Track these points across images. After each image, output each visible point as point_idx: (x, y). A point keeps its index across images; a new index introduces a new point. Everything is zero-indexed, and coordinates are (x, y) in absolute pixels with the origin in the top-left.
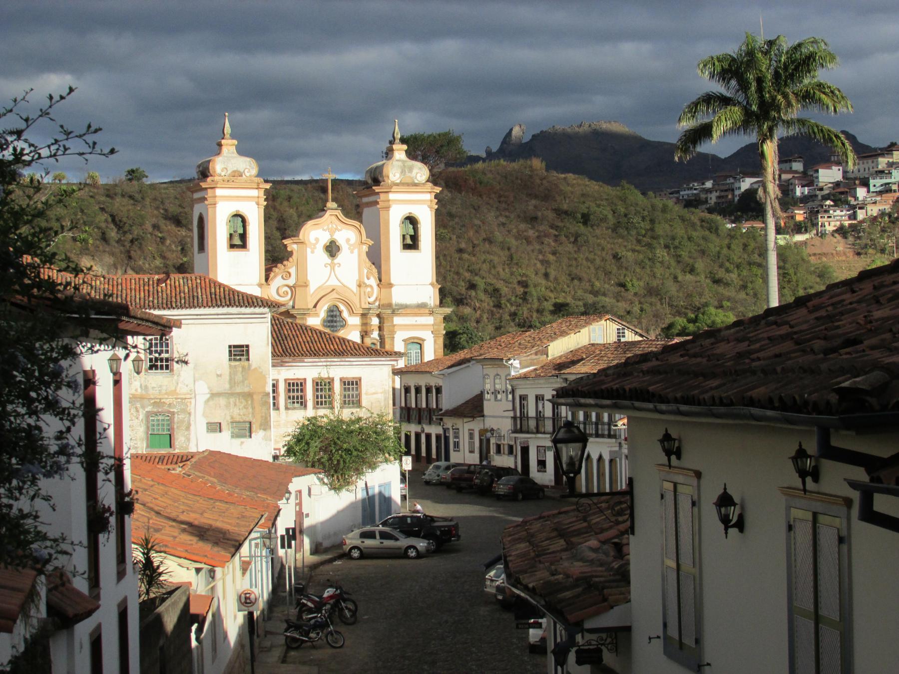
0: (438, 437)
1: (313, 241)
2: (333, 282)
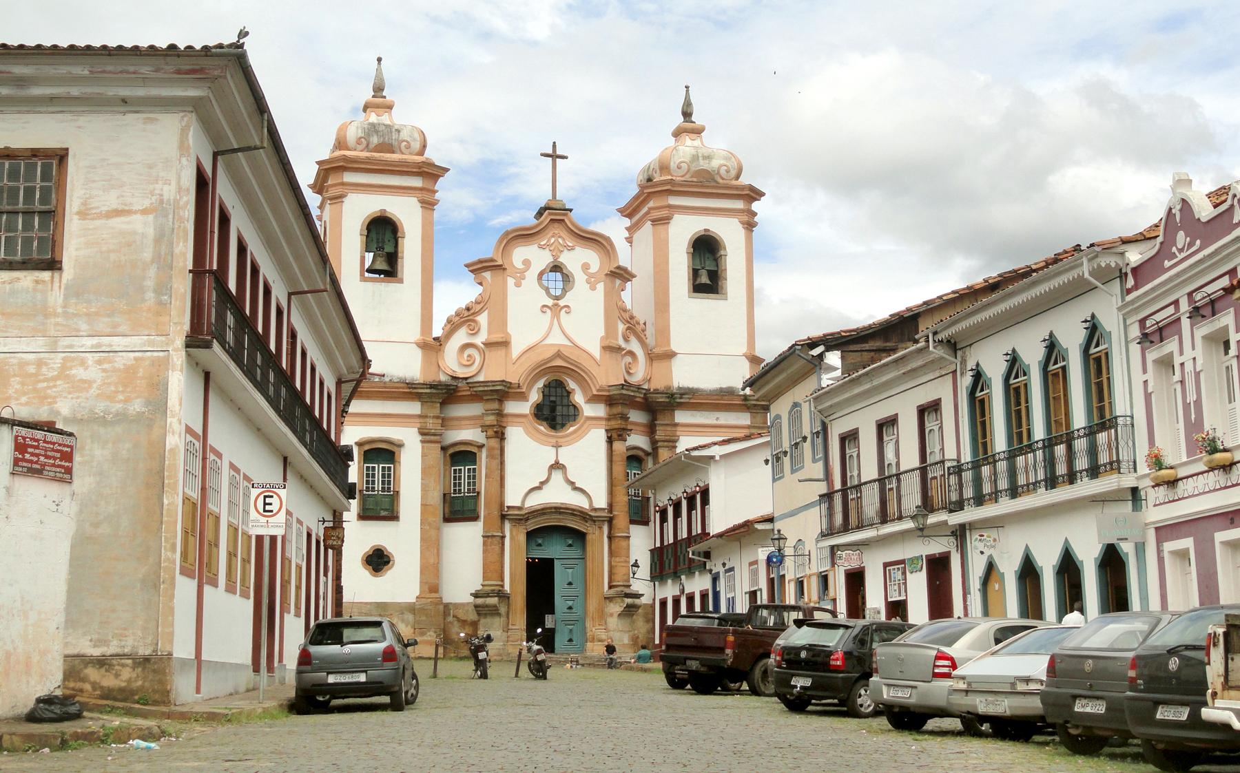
0: (704, 596)
1: (518, 264)
2: (556, 339)
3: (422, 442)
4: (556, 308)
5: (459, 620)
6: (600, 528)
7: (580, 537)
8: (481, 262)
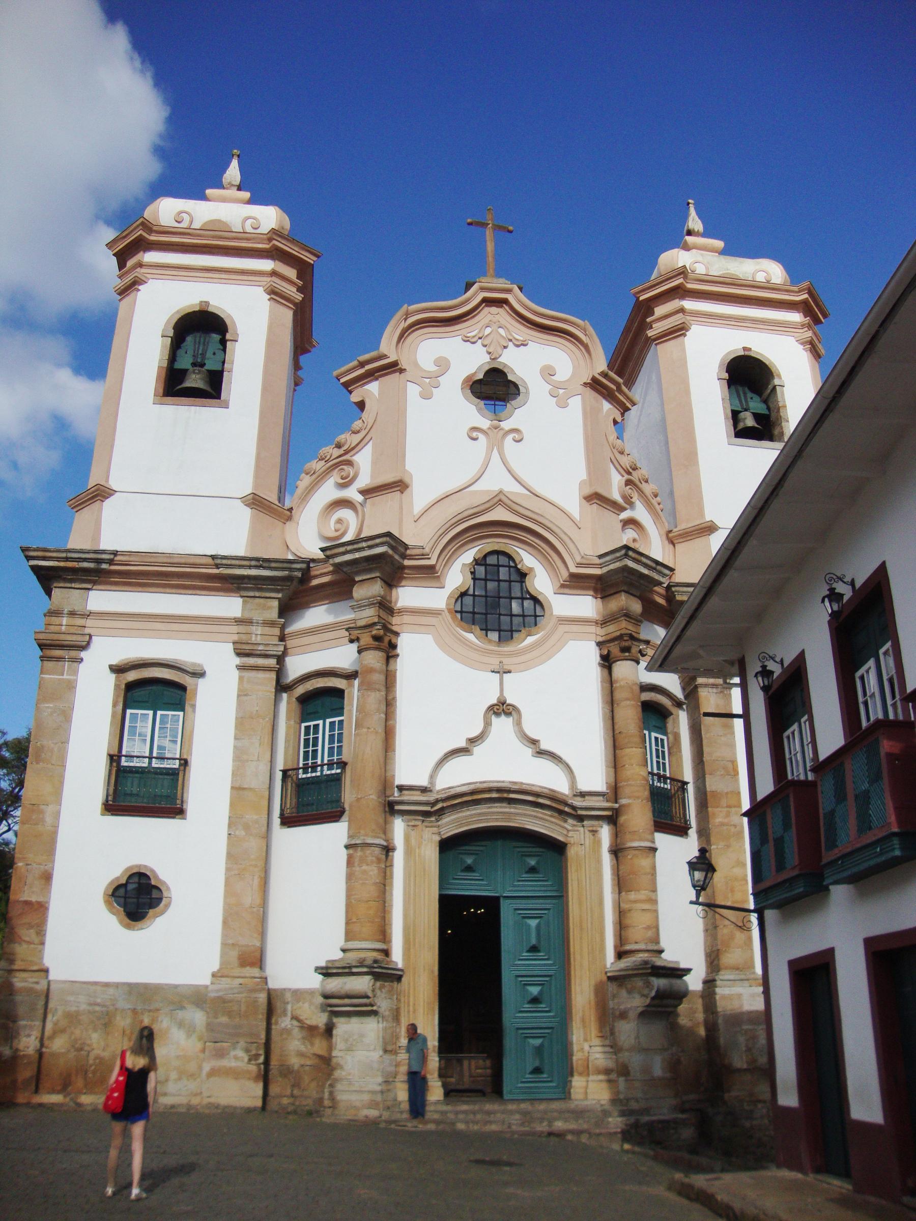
2: (496, 481)
3: (241, 668)
6: (594, 832)
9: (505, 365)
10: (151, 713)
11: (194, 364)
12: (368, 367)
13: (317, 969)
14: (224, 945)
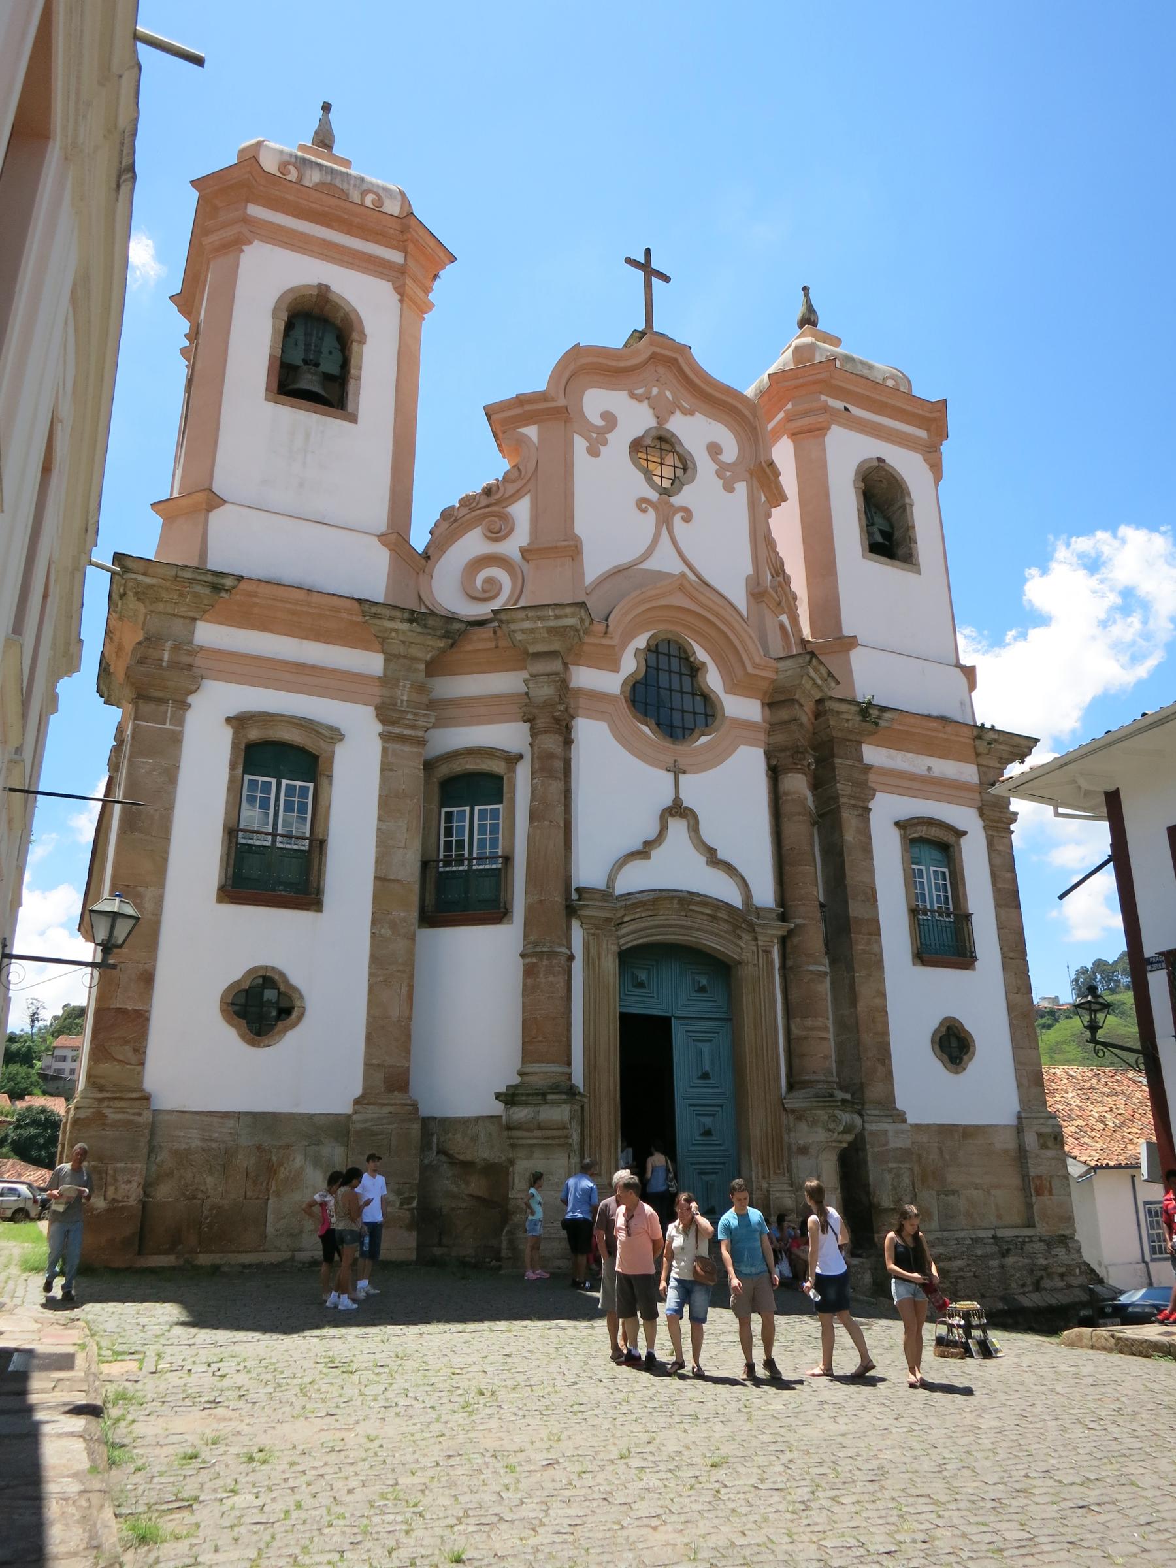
4: (665, 509)
5: (453, 1161)
7: (721, 969)
8: (520, 400)
9: (673, 435)
10: (274, 781)
11: (306, 362)
12: (527, 407)
13: (498, 1096)
14: (368, 1065)
